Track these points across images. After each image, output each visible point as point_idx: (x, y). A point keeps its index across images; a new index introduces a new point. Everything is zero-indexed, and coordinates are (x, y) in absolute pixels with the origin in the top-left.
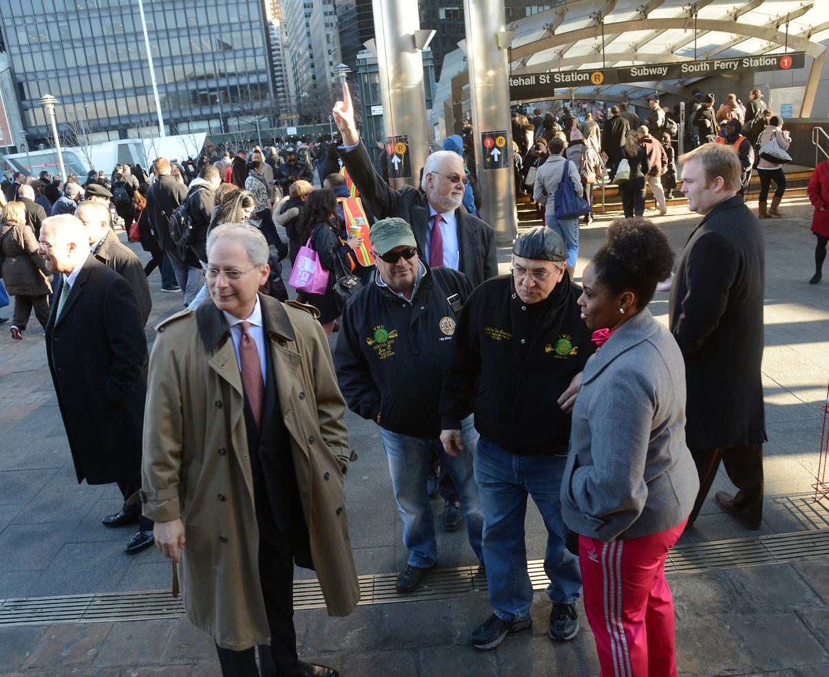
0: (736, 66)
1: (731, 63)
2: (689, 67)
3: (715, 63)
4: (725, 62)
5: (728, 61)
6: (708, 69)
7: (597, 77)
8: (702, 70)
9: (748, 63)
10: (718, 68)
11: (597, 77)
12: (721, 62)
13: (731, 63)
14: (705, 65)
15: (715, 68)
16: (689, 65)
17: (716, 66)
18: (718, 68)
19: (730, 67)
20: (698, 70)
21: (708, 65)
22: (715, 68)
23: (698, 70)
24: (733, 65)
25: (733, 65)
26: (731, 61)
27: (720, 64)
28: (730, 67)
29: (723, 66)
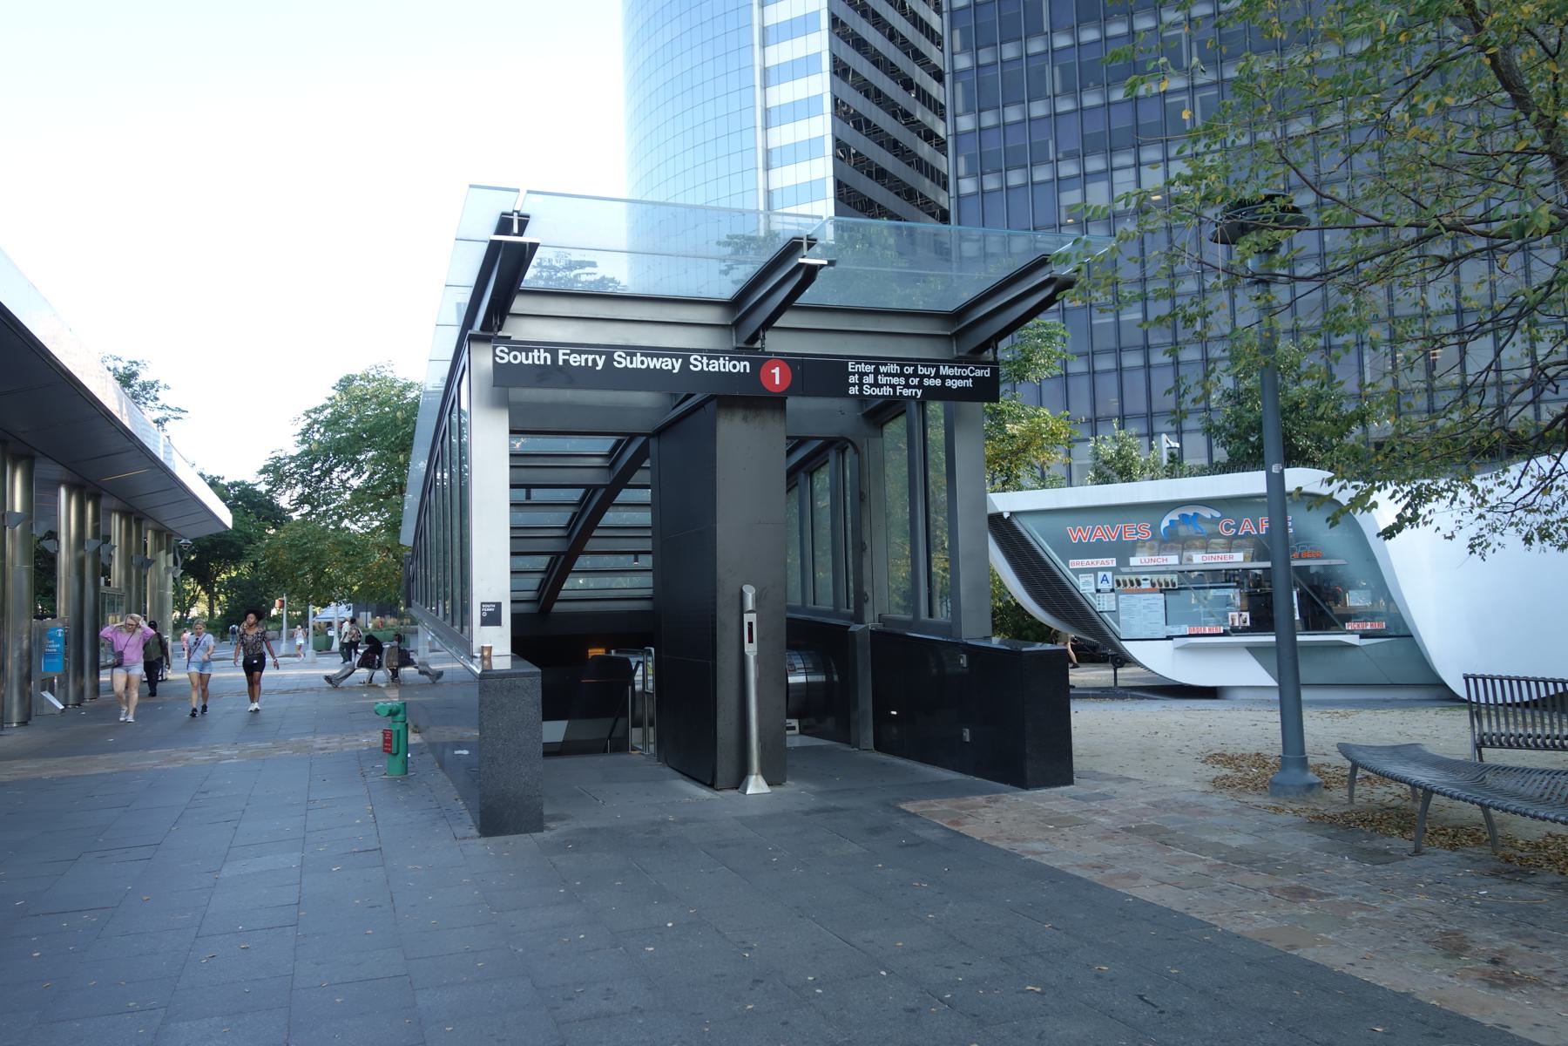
0: (601, 363)
3: (561, 352)
6: (549, 362)
8: (537, 362)
12: (573, 352)
14: (543, 355)
15: (561, 363)
16: (511, 350)
17: (561, 358)
19: (590, 364)
22: (561, 363)
23: (530, 361)
24: (594, 360)
25: (594, 361)
27: (569, 355)
28: (590, 364)
29: (576, 360)
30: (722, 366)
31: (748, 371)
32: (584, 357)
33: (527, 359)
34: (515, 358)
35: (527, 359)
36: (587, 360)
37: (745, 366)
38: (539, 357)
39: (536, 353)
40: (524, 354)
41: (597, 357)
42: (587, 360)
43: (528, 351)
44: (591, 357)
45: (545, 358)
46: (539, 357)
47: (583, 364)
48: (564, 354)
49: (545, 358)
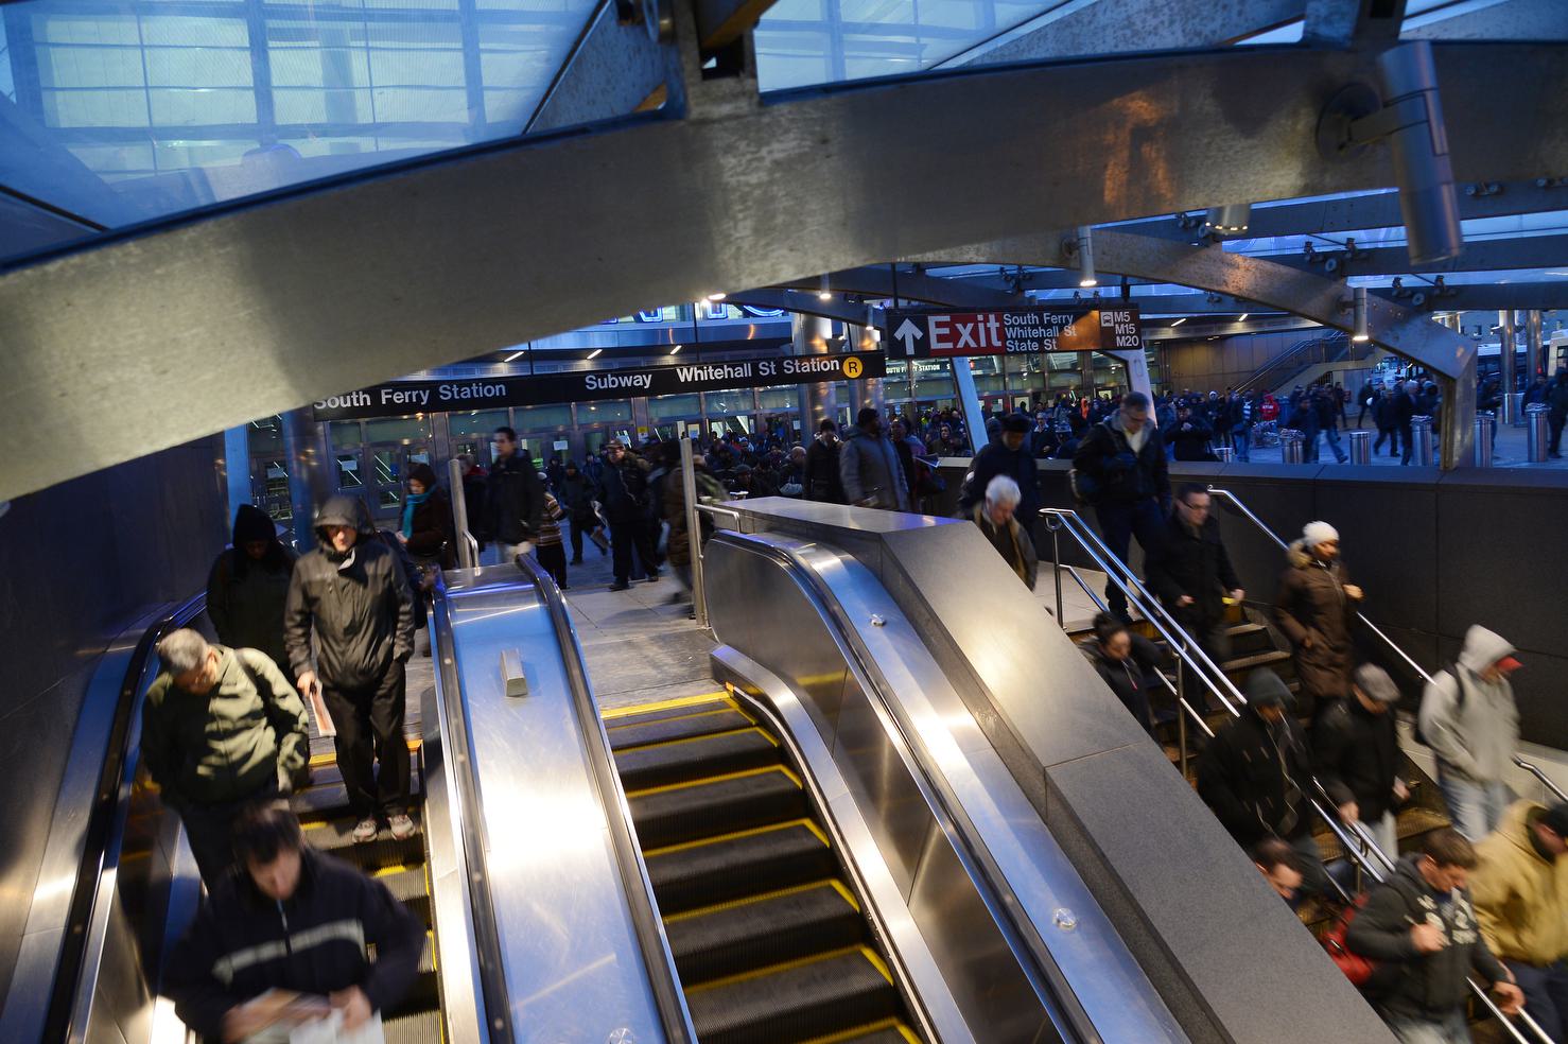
2: (329, 401)
7: (853, 365)
9: (450, 394)
11: (853, 365)
13: (414, 393)
15: (384, 403)
19: (414, 400)
20: (349, 405)
22: (384, 403)
24: (418, 396)
25: (418, 396)
27: (392, 394)
28: (414, 400)
30: (475, 391)
31: (504, 394)
32: (407, 394)
33: (345, 402)
35: (345, 402)
36: (410, 396)
37: (500, 389)
38: (358, 402)
40: (342, 398)
41: (421, 392)
42: (410, 396)
44: (414, 393)
45: (365, 399)
46: (358, 402)
47: (407, 401)
48: (386, 394)
49: (365, 399)
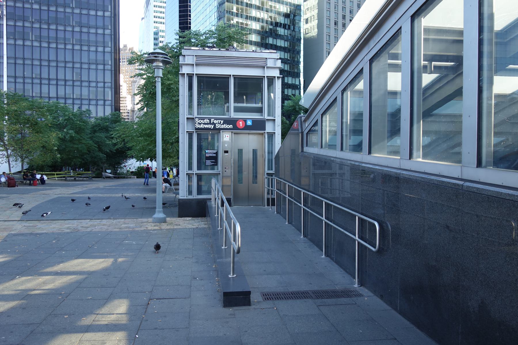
1: (219, 121)
2: (200, 120)
3: (212, 120)
4: (217, 120)
5: (218, 120)
10: (213, 122)
12: (215, 120)
14: (207, 120)
15: (212, 122)
16: (199, 119)
17: (212, 121)
18: (213, 122)
21: (209, 121)
22: (212, 122)
25: (220, 122)
26: (220, 120)
34: (200, 121)
36: (218, 122)
39: (205, 120)
42: (218, 122)
43: (203, 120)
